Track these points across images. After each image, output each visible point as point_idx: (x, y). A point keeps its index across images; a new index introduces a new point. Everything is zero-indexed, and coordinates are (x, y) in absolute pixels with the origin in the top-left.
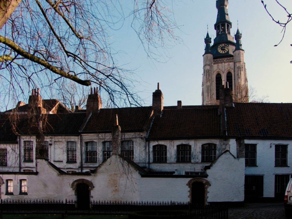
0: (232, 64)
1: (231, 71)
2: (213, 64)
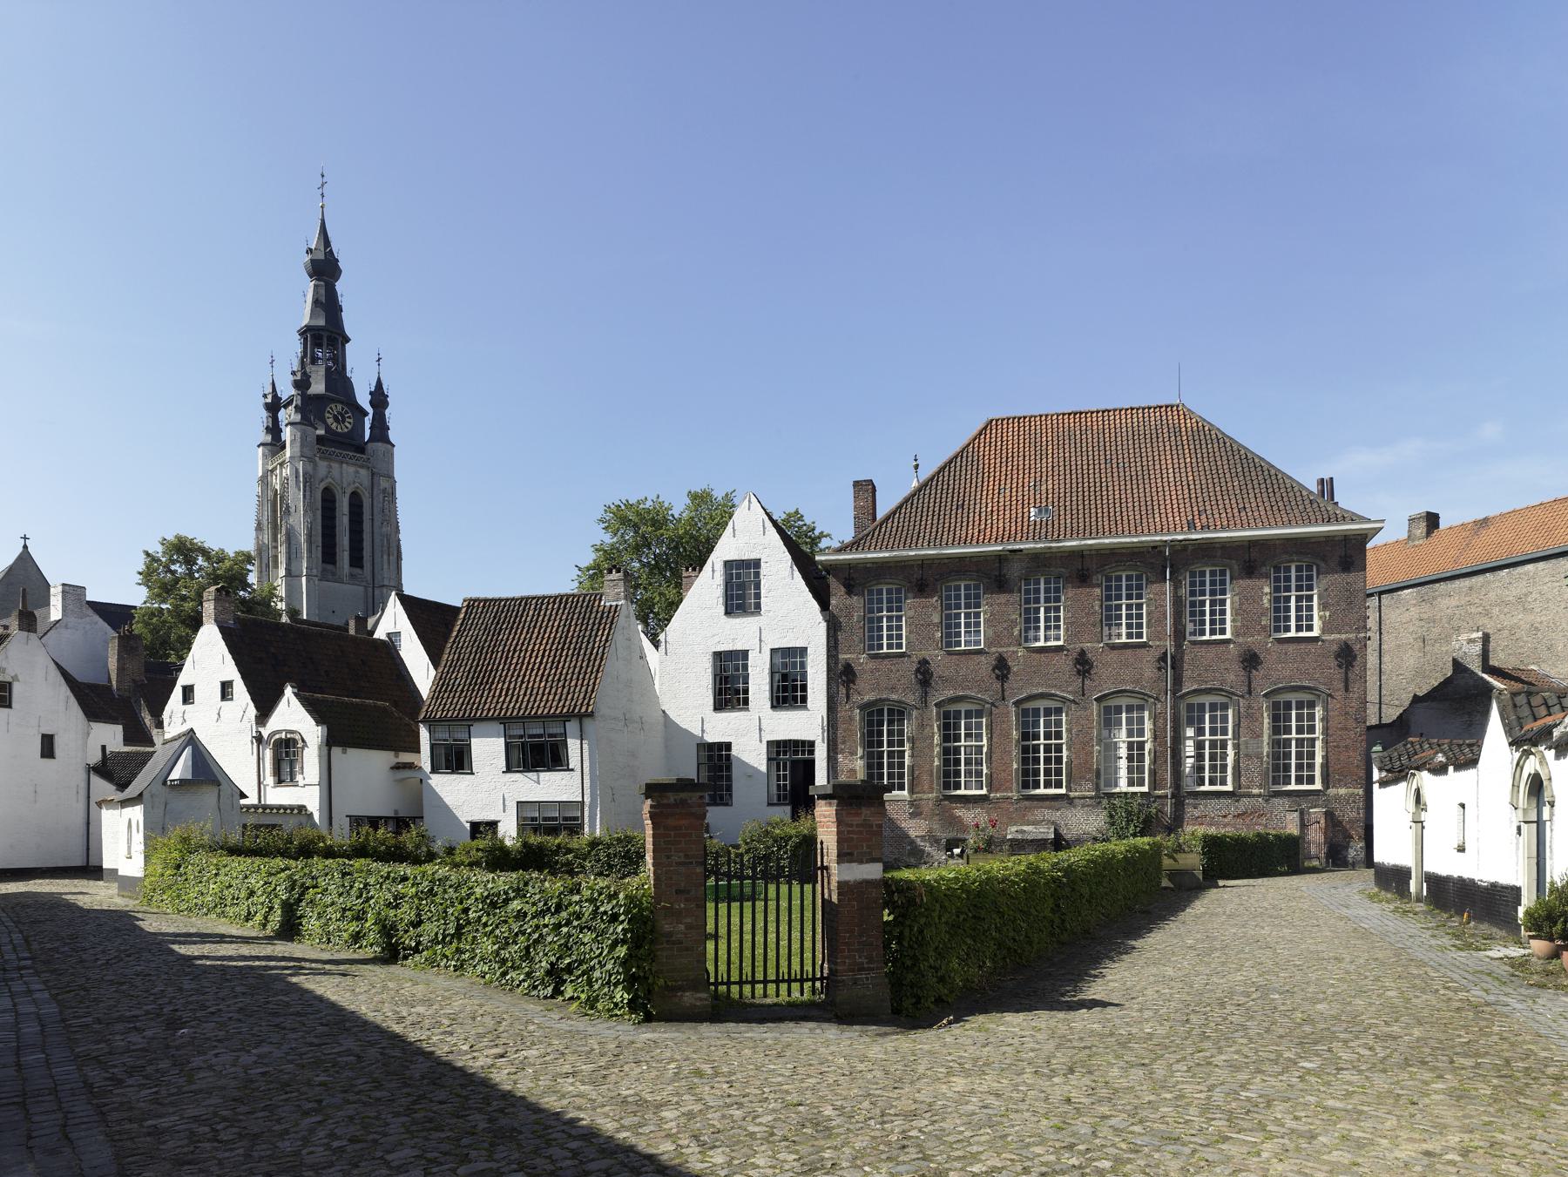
0: (363, 472)
2: (317, 459)
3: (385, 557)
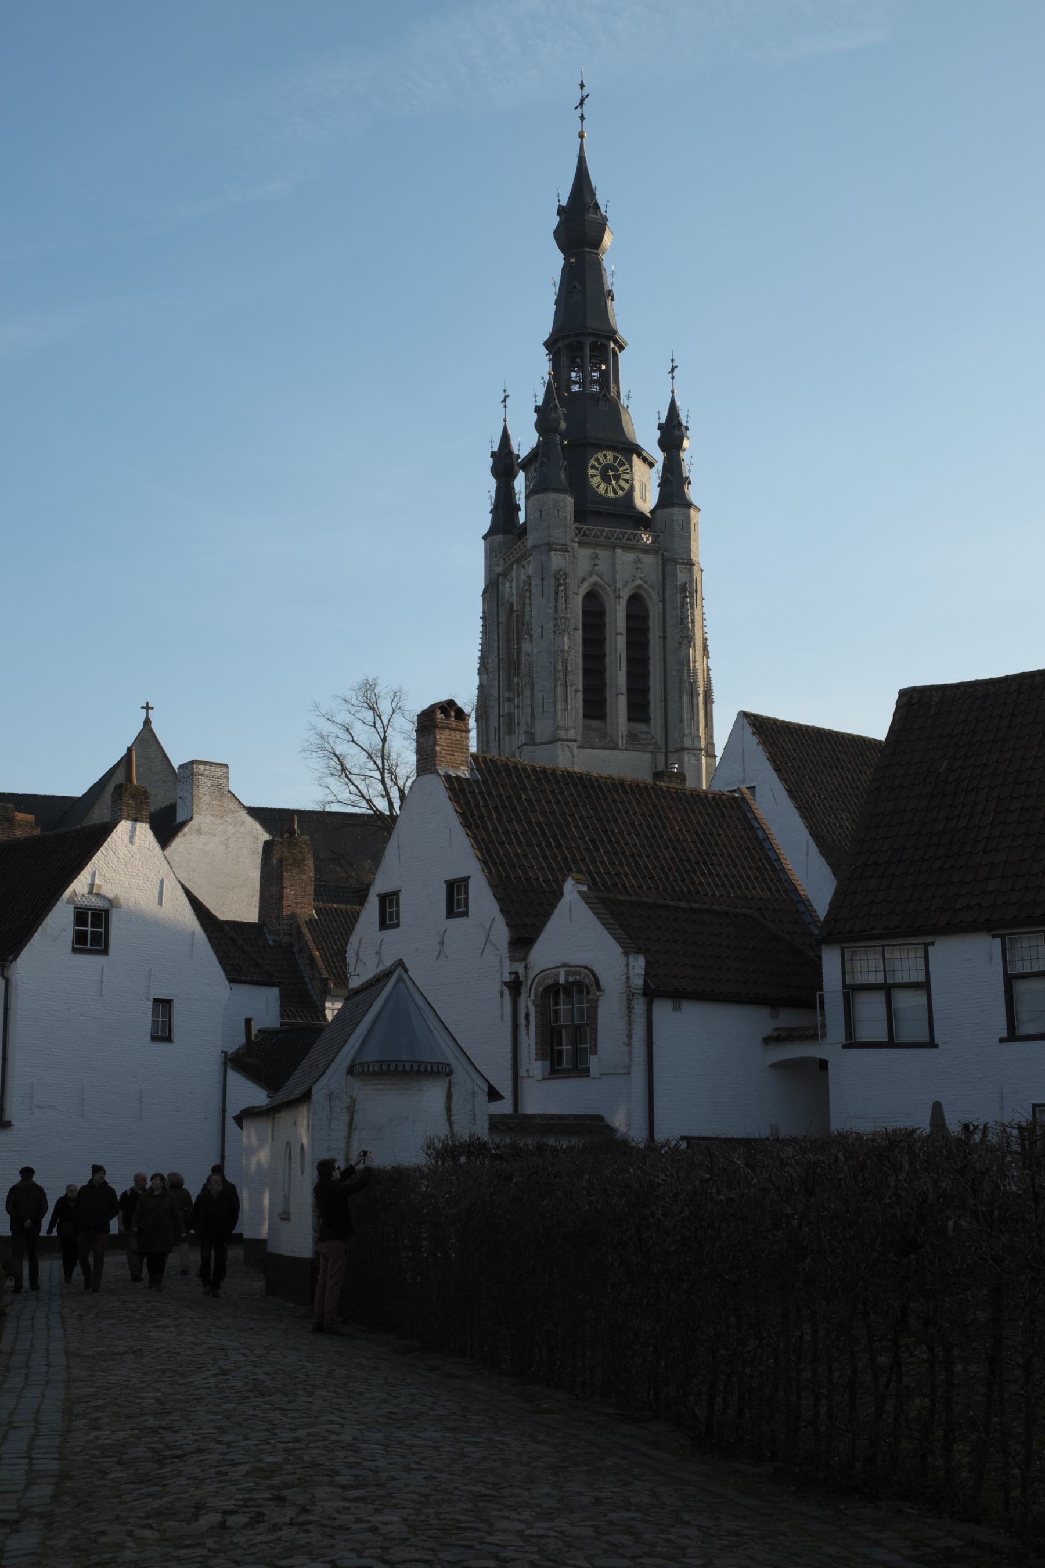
0: (648, 559)
1: (642, 592)
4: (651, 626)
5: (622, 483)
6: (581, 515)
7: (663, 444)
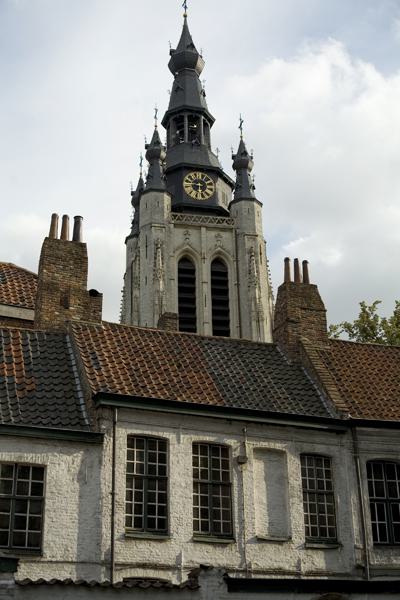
0: (226, 236)
3: (254, 324)
4: (229, 278)
5: (207, 191)
6: (175, 209)
7: (234, 167)
